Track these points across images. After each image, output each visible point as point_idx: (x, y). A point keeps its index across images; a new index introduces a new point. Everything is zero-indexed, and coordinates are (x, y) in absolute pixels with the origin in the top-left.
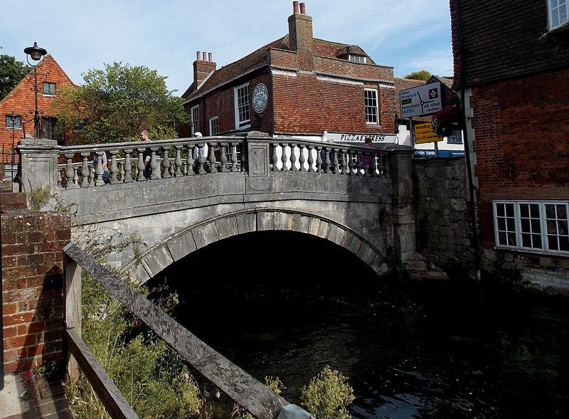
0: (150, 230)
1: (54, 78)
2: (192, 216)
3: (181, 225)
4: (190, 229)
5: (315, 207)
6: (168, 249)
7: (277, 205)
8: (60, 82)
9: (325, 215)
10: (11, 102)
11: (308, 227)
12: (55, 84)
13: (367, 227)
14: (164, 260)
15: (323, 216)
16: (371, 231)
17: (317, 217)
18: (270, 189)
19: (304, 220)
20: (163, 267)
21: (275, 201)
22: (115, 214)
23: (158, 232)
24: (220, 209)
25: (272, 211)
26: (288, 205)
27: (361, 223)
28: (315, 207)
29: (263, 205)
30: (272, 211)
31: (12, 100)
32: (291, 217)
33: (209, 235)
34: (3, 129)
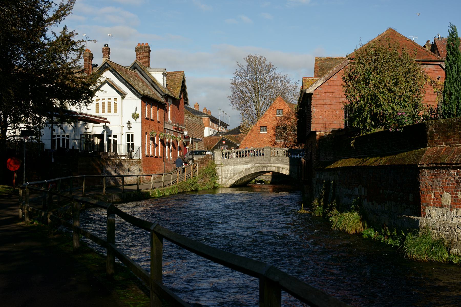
0: (239, 168)
2: (249, 166)
3: (246, 168)
4: (249, 169)
7: (272, 165)
8: (284, 108)
10: (262, 120)
11: (282, 171)
14: (242, 175)
19: (281, 169)
20: (242, 177)
26: (276, 165)
30: (271, 166)
31: (263, 119)
32: (277, 168)
33: (253, 171)
34: (259, 133)
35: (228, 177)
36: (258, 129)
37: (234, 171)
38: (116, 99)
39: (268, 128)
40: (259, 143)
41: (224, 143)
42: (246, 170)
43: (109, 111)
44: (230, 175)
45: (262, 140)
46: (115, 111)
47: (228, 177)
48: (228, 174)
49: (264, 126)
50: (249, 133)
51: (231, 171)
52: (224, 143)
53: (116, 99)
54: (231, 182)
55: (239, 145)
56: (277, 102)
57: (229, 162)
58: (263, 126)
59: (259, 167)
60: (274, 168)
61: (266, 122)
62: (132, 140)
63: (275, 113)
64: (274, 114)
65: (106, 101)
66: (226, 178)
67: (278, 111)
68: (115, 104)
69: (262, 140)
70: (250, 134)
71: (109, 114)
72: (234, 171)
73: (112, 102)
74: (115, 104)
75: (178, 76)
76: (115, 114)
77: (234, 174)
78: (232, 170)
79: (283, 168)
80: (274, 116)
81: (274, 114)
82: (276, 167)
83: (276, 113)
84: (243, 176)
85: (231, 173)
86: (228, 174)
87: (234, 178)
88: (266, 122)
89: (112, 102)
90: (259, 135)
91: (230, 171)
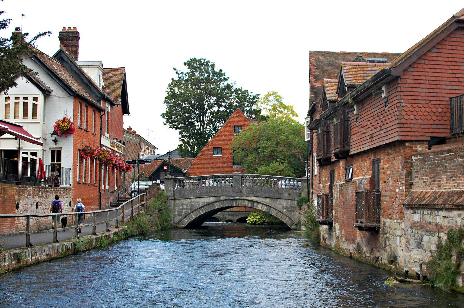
1: (241, 123)
2: (212, 199)
4: (211, 203)
5: (260, 200)
6: (204, 209)
7: (244, 198)
8: (244, 125)
9: (265, 203)
10: (216, 140)
11: (257, 206)
12: (242, 126)
13: (286, 209)
14: (203, 211)
15: (264, 203)
16: (288, 211)
17: (261, 203)
18: (241, 192)
19: (255, 204)
20: (202, 213)
21: (243, 196)
22: (188, 197)
23: (201, 203)
24: (222, 198)
25: (242, 199)
26: (248, 198)
27: (283, 207)
28: (260, 200)
29: (238, 197)
31: (217, 138)
33: (217, 206)
35: (182, 214)
36: (210, 151)
37: (192, 206)
38: (35, 99)
39: (223, 150)
40: (211, 169)
41: (165, 168)
42: (208, 204)
43: (25, 114)
44: (186, 211)
45: (215, 165)
46: (35, 114)
47: (182, 214)
48: (183, 209)
49: (218, 146)
50: (199, 156)
51: (187, 206)
52: (165, 168)
53: (35, 99)
54: (187, 221)
55: (185, 171)
56: (236, 116)
57: (184, 193)
58: (217, 146)
59: (226, 200)
60: (247, 202)
61: (220, 143)
62: (59, 160)
63: (232, 131)
64: (231, 132)
65: (21, 101)
66: (180, 215)
67: (236, 128)
68: (35, 106)
69: (215, 165)
70: (200, 157)
71: (25, 120)
72: (192, 206)
73: (30, 102)
74: (35, 106)
75: (117, 74)
76: (34, 120)
77: (191, 209)
78: (188, 204)
79: (258, 203)
80: (231, 135)
81: (231, 132)
82: (249, 201)
83: (233, 131)
84: (204, 213)
85: (186, 209)
86: (183, 209)
87: (191, 215)
88: (220, 143)
89: (30, 102)
90: (211, 159)
91: (185, 206)
